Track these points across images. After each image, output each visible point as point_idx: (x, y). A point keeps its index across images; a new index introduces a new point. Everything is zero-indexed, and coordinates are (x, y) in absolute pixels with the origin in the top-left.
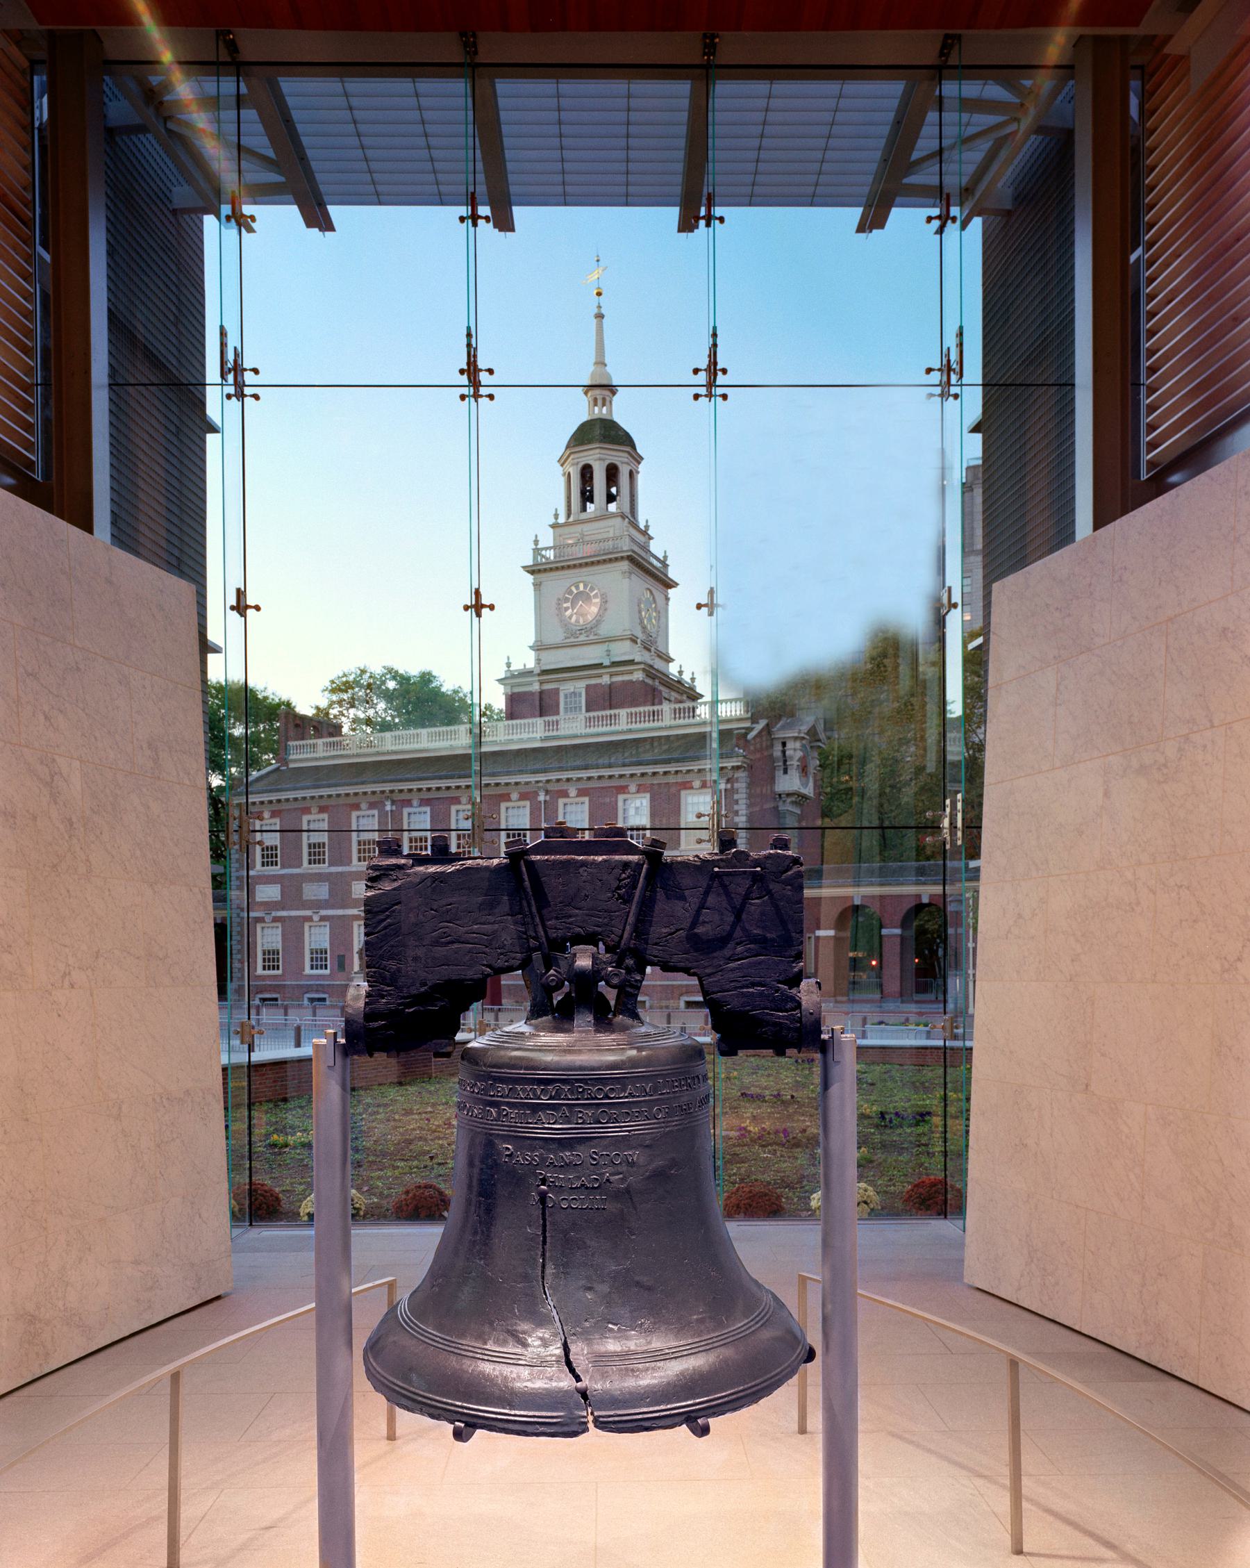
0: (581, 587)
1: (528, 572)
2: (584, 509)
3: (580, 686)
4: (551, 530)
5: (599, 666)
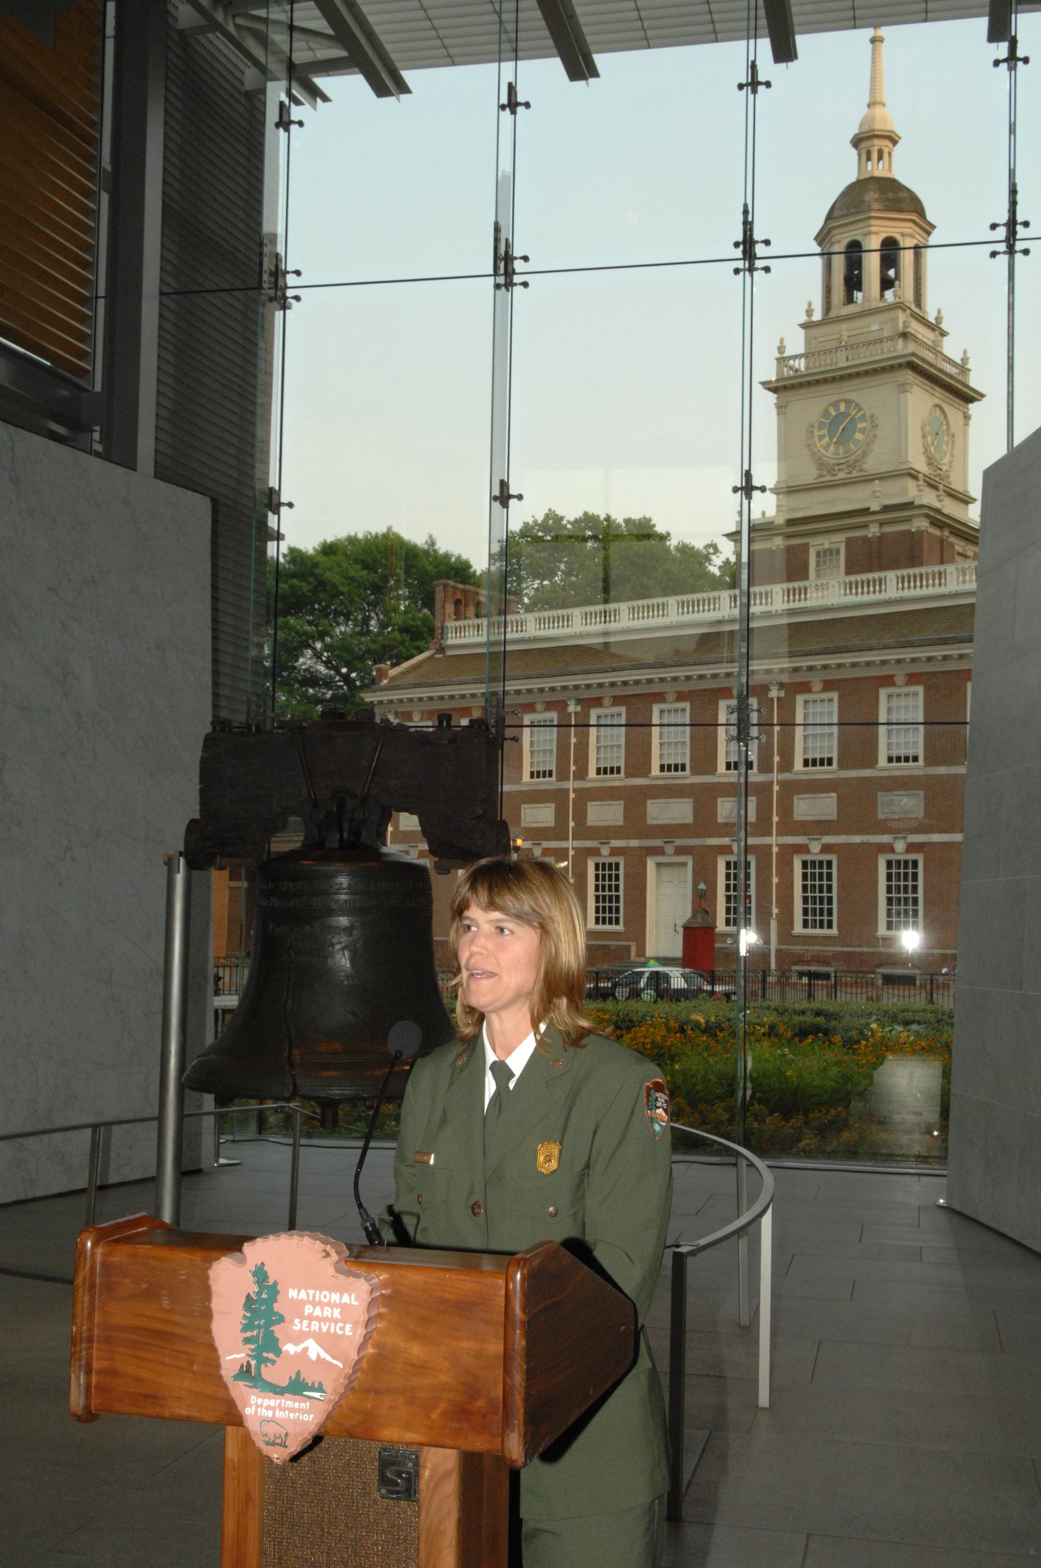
0: (842, 407)
1: (770, 389)
2: (850, 300)
3: (838, 541)
4: (802, 332)
5: (865, 511)
